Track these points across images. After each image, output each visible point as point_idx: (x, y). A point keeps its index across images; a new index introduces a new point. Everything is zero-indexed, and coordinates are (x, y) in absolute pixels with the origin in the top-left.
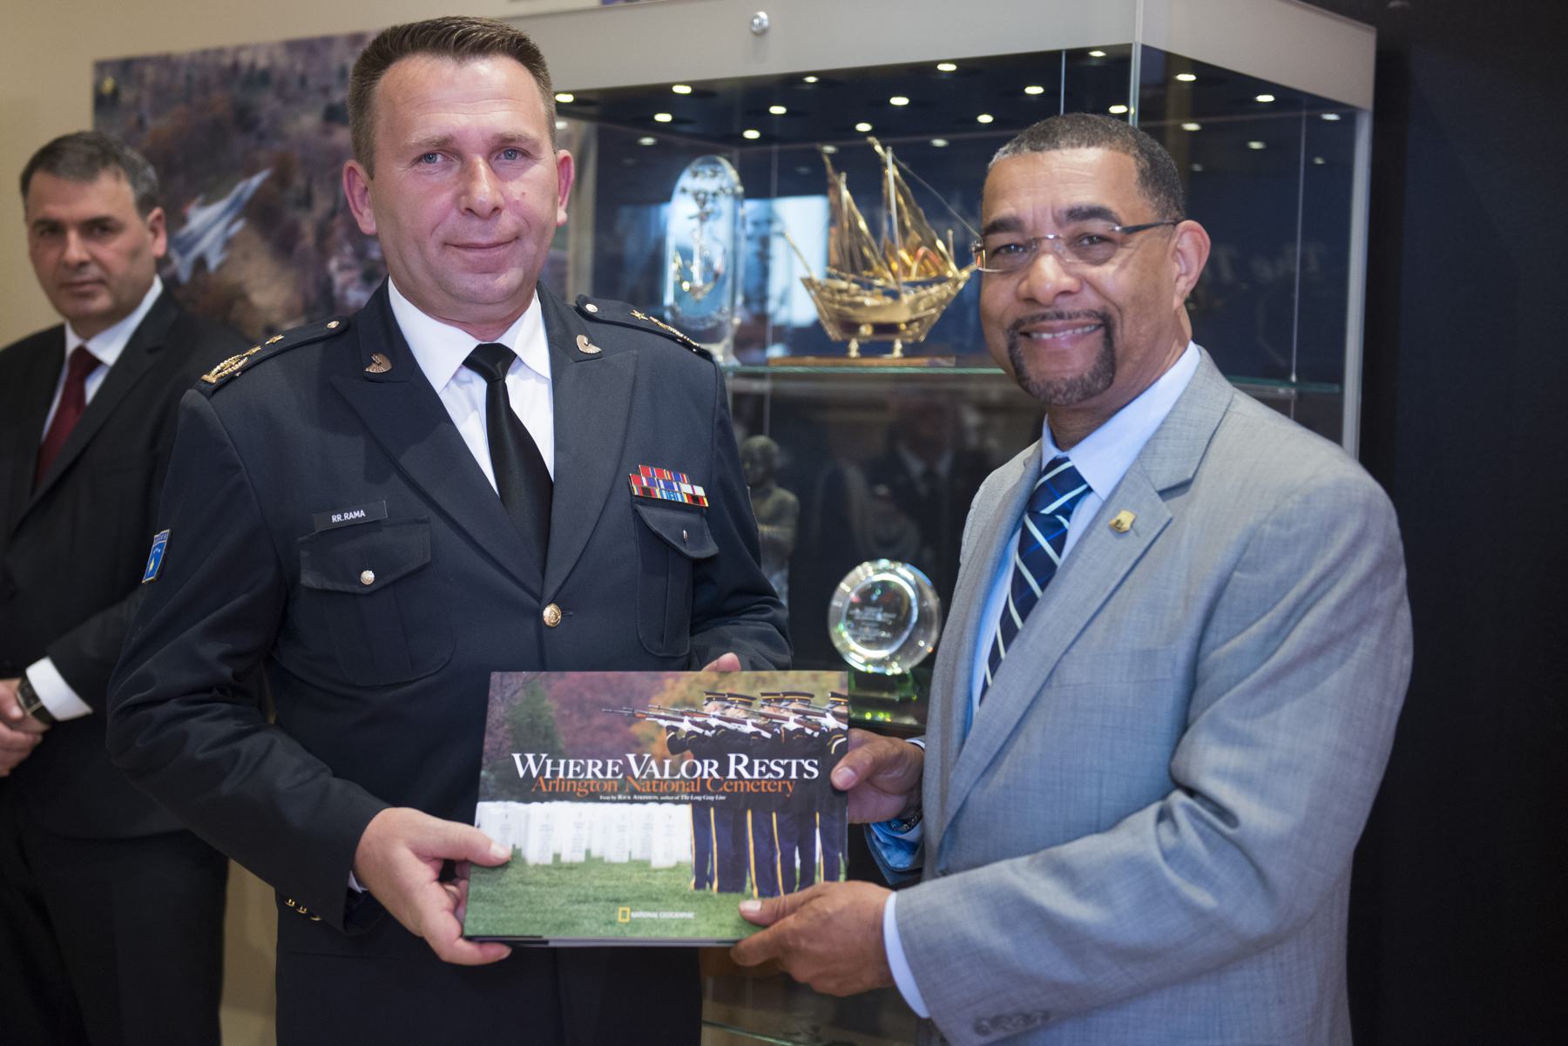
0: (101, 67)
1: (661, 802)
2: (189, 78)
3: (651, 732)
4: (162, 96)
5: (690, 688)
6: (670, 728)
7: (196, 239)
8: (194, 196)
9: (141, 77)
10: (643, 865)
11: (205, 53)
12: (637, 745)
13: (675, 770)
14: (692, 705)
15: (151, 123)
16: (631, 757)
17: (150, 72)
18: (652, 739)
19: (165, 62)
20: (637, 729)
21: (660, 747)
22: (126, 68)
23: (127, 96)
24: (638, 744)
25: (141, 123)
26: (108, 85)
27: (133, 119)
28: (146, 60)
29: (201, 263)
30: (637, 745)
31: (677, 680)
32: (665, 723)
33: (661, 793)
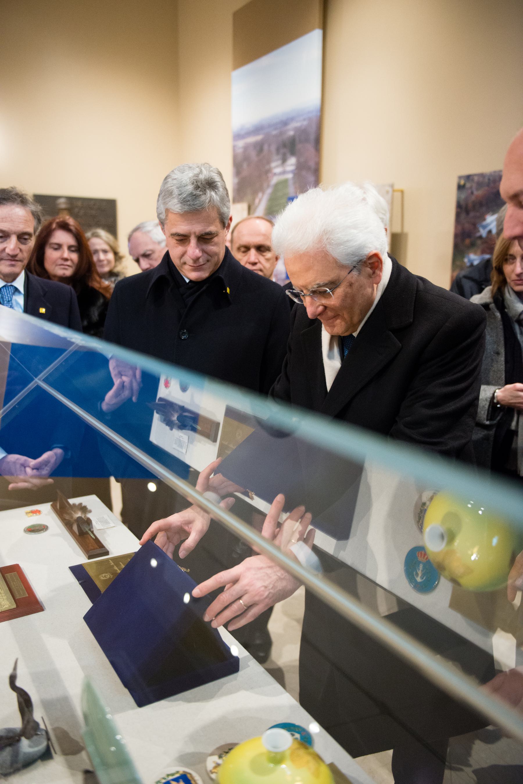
0: (460, 178)
2: (489, 179)
4: (480, 185)
7: (488, 225)
8: (489, 212)
9: (473, 180)
11: (495, 172)
15: (476, 193)
17: (476, 178)
19: (482, 175)
22: (468, 177)
23: (468, 185)
25: (472, 193)
26: (462, 182)
27: (470, 191)
28: (475, 175)
29: (490, 232)
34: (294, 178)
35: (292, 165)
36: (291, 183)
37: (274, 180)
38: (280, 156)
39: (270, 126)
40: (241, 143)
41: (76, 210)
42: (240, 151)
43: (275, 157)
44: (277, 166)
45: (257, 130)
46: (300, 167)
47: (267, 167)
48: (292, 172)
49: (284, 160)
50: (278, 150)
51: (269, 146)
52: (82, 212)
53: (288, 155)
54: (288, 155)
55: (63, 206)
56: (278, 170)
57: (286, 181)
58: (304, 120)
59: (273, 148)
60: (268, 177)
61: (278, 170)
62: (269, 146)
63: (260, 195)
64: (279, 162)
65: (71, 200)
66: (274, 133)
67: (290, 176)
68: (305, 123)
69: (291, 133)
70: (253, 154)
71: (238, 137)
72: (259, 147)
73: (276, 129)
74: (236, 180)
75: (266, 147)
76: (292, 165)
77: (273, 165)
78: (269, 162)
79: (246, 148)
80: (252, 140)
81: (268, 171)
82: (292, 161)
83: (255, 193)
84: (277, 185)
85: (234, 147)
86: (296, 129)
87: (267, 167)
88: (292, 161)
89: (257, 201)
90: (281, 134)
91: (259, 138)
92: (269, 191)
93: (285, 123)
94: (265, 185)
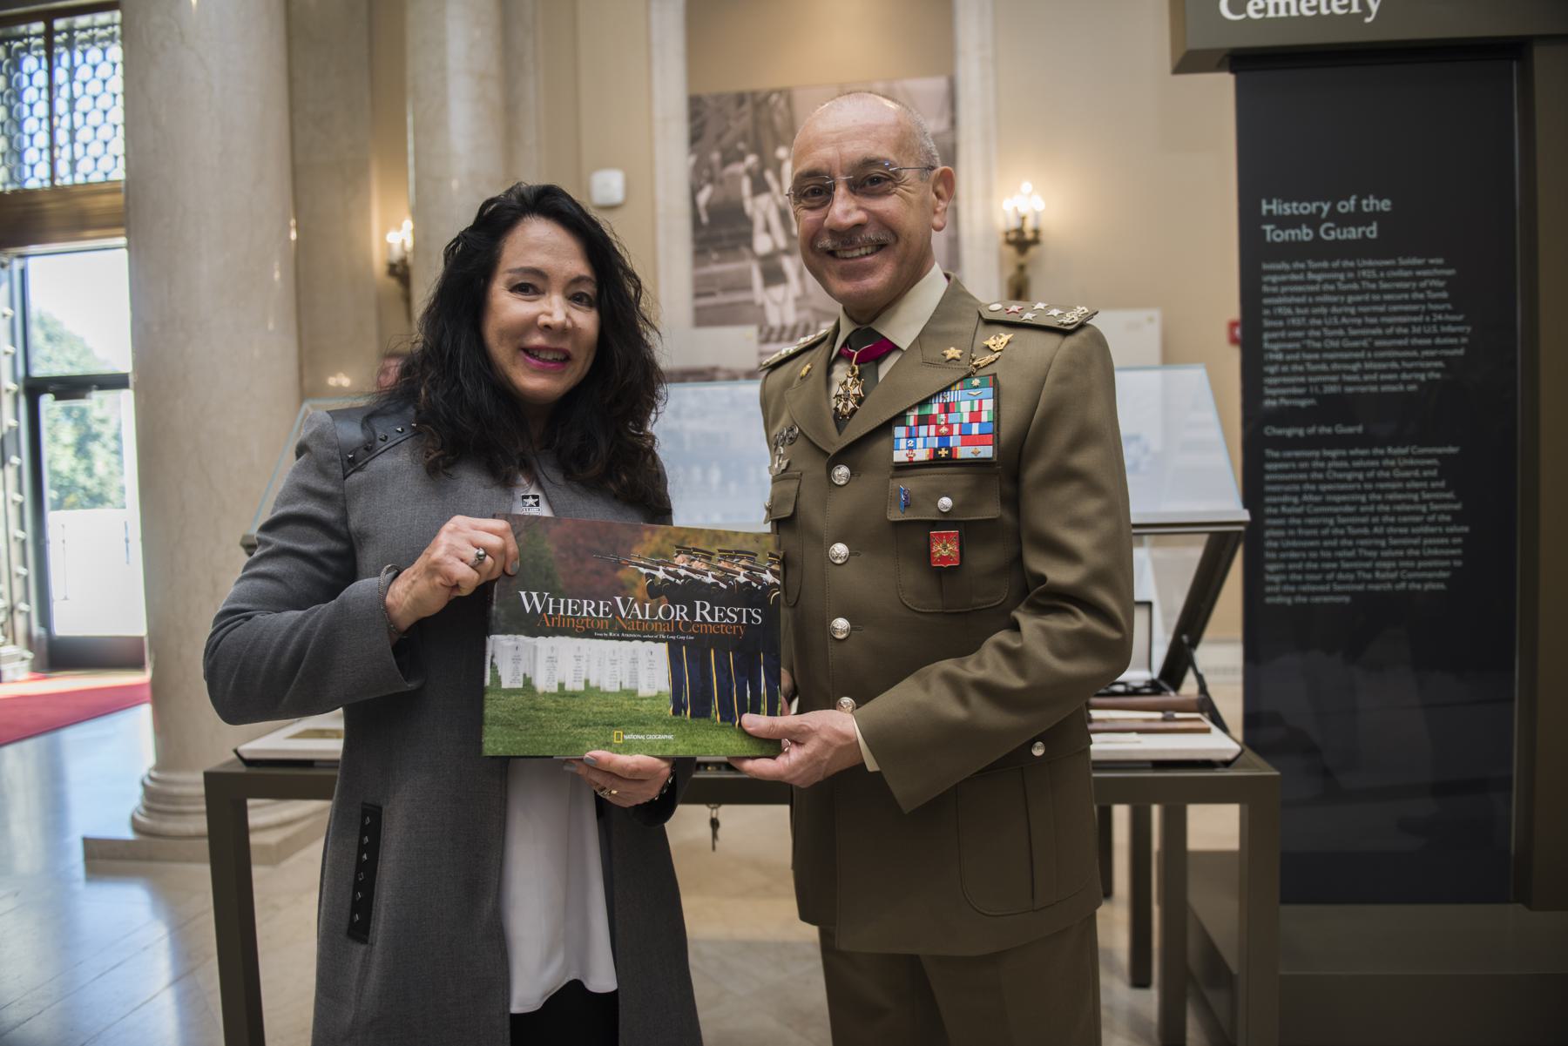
1: (644, 640)
3: (633, 577)
5: (663, 541)
6: (649, 576)
10: (632, 694)
12: (623, 589)
13: (654, 613)
14: (666, 556)
16: (618, 599)
18: (635, 585)
20: (622, 575)
21: (640, 591)
24: (623, 588)
30: (623, 589)
31: (653, 531)
32: (645, 571)
33: (644, 633)
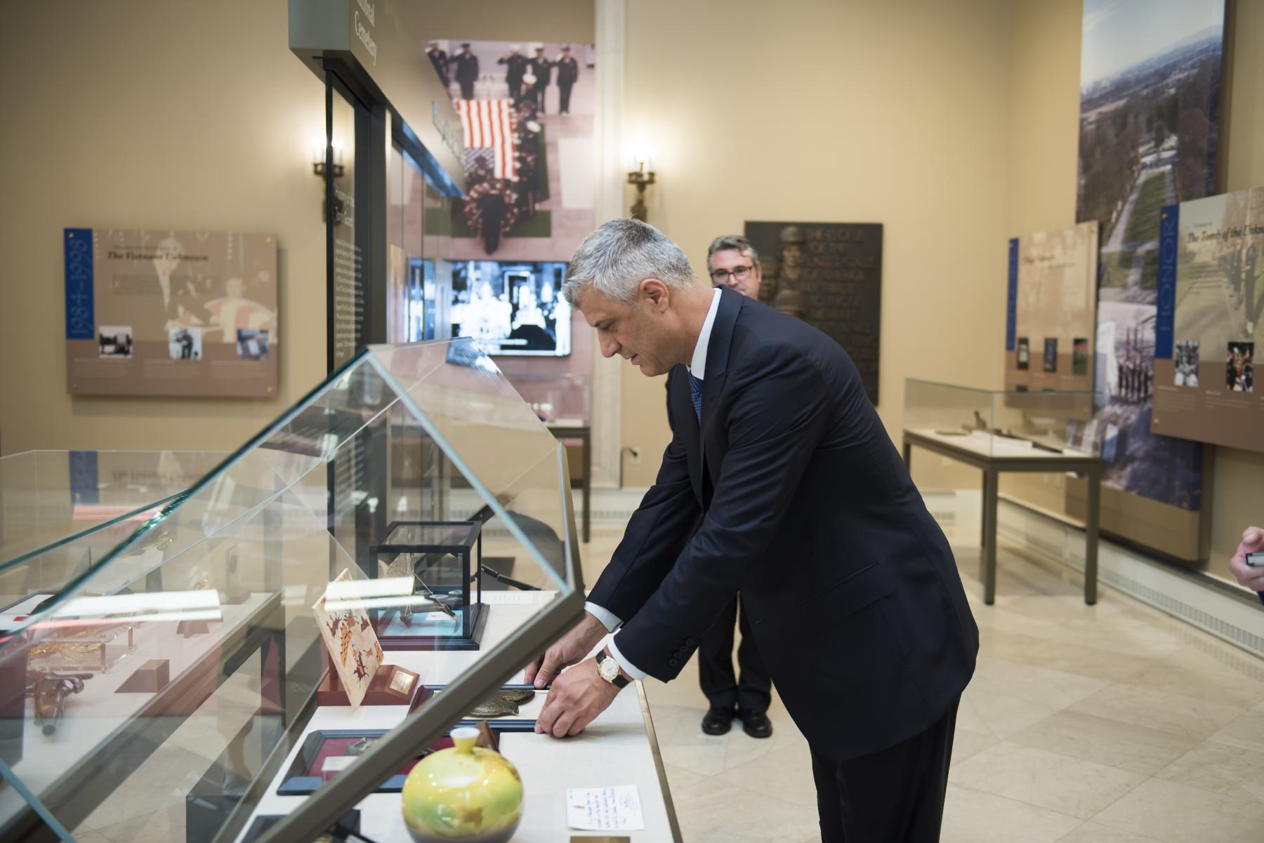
34: (1173, 170)
35: (1172, 148)
36: (1168, 180)
37: (1143, 177)
38: (1153, 135)
39: (1139, 81)
40: (1092, 115)
41: (812, 246)
42: (1092, 127)
43: (1147, 137)
44: (1147, 154)
45: (1119, 88)
46: (1183, 150)
47: (1132, 155)
48: (1170, 161)
49: (1159, 141)
50: (1149, 122)
51: (1137, 116)
52: (821, 248)
53: (1166, 132)
54: (1166, 132)
55: (791, 239)
56: (1148, 160)
57: (1162, 175)
58: (1193, 67)
59: (1143, 119)
60: (1133, 172)
61: (1148, 160)
62: (1137, 116)
63: (1120, 204)
64: (1153, 144)
65: (805, 228)
66: (1145, 92)
67: (1169, 167)
68: (1195, 71)
69: (1172, 91)
70: (1111, 133)
71: (1088, 103)
72: (1120, 119)
73: (1146, 87)
74: (1083, 182)
75: (1131, 119)
76: (1172, 148)
77: (1142, 150)
78: (1135, 146)
79: (1100, 122)
80: (1108, 108)
81: (1135, 161)
82: (1172, 141)
83: (1111, 203)
84: (1146, 184)
85: (1082, 121)
86: (1180, 84)
87: (1132, 155)
88: (1172, 141)
89: (1114, 215)
90: (1156, 93)
91: (1121, 103)
92: (1133, 197)
93: (1162, 74)
94: (1128, 187)
